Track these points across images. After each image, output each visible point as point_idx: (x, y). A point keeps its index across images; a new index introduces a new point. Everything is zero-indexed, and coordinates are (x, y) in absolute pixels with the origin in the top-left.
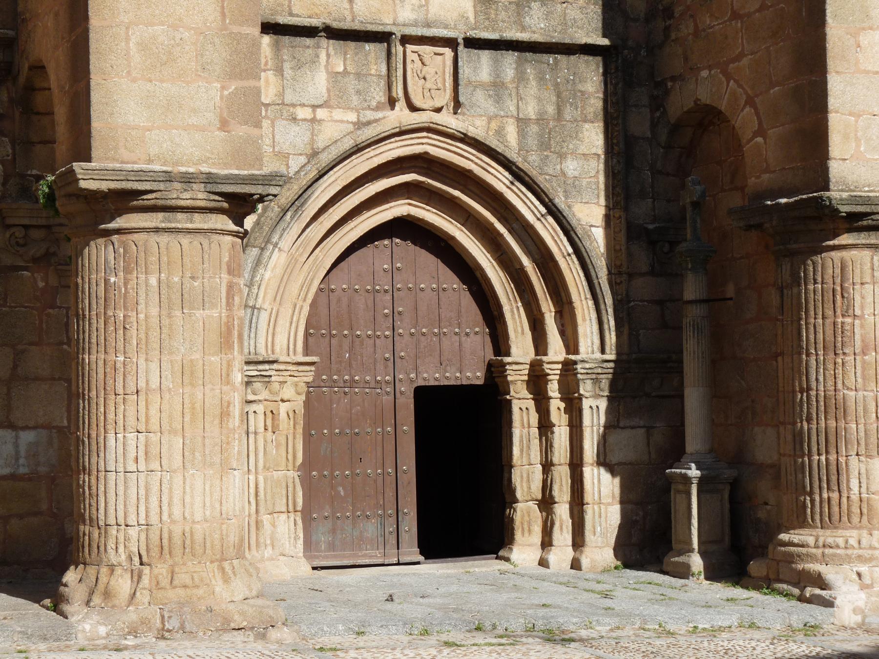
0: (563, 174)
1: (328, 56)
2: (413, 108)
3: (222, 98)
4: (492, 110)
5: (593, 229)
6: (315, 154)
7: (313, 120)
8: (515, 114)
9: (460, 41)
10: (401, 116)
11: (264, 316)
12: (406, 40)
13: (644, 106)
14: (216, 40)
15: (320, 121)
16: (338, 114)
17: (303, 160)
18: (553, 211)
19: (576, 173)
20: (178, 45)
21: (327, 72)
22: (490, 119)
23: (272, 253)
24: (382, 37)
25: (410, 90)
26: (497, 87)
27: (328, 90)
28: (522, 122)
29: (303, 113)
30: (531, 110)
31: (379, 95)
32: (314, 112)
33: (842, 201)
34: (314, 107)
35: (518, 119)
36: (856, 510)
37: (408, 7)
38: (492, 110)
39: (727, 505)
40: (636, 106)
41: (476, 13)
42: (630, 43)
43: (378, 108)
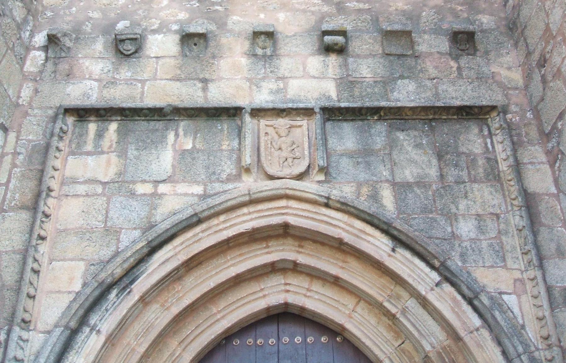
1: (177, 135)
4: (363, 176)
5: (505, 297)
7: (155, 195)
8: (390, 178)
9: (317, 110)
10: (252, 184)
12: (257, 112)
13: (542, 163)
15: (161, 196)
16: (182, 188)
18: (448, 277)
19: (473, 235)
21: (175, 150)
22: (360, 185)
23: (88, 337)
24: (232, 113)
25: (263, 159)
26: (364, 154)
27: (173, 166)
28: (401, 188)
29: (142, 189)
30: (408, 174)
31: (228, 168)
32: (156, 187)
34: (157, 183)
35: (394, 184)
38: (363, 176)
40: (531, 163)
41: (339, 92)
42: (513, 108)
43: (229, 179)
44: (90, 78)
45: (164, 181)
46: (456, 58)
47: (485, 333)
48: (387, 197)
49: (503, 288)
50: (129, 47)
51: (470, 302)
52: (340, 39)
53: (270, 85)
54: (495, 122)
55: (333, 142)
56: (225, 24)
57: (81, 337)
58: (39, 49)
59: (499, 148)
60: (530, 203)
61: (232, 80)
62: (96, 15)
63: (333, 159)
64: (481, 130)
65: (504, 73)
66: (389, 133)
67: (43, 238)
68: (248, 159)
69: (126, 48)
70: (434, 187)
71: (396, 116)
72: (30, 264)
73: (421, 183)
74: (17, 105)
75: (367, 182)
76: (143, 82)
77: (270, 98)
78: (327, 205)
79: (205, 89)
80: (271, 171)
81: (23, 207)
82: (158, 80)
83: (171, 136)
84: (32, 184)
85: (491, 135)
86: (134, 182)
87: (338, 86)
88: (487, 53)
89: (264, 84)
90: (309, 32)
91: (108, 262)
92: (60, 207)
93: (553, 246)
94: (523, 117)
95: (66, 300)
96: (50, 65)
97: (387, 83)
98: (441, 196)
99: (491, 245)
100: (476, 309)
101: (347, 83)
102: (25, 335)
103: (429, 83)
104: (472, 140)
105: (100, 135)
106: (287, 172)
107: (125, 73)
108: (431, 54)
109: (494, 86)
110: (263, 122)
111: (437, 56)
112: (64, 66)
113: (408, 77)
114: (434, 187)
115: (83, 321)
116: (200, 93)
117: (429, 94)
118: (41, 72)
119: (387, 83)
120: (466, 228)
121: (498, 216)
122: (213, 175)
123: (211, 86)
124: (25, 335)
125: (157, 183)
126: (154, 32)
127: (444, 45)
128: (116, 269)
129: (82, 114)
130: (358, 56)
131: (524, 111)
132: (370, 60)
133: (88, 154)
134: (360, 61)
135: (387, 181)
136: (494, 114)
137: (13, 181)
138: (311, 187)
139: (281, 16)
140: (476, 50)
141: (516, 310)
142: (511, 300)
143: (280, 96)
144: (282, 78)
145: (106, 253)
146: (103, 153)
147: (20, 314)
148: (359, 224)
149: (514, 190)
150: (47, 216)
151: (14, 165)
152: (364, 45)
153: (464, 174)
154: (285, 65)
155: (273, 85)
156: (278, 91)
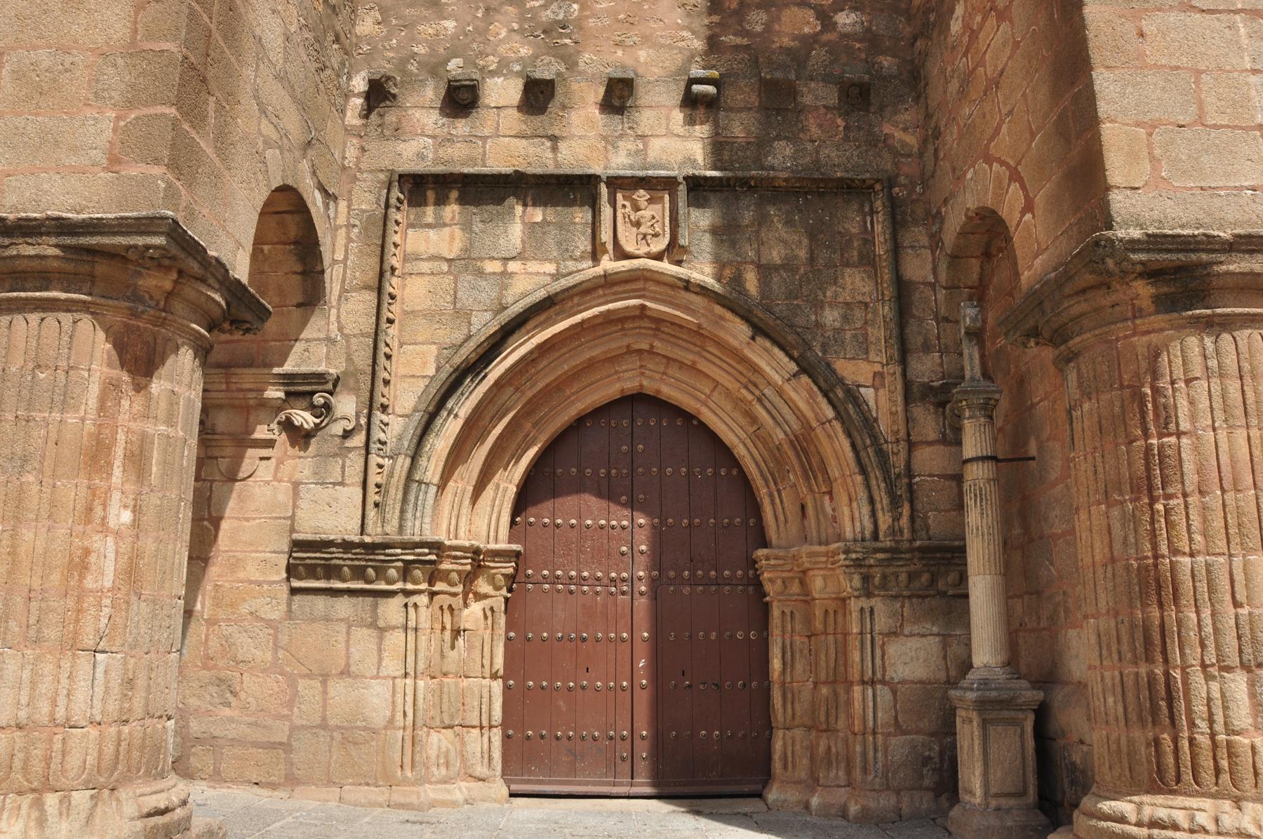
0: (818, 324)
2: (621, 254)
3: (115, 130)
5: (862, 390)
7: (504, 274)
8: (756, 259)
9: (680, 180)
13: (924, 247)
14: (120, 61)
15: (511, 275)
16: (533, 266)
18: (806, 368)
19: (837, 325)
20: (66, 71)
21: (524, 223)
23: (446, 420)
25: (620, 235)
27: (523, 242)
28: (765, 271)
30: (775, 255)
31: (584, 244)
32: (505, 265)
33: (1133, 245)
34: (506, 260)
36: (1207, 762)
37: (623, 153)
38: (726, 256)
39: (1030, 744)
40: (912, 247)
42: (902, 179)
46: (846, 115)
47: (837, 425)
48: (751, 282)
49: (862, 380)
50: (464, 96)
51: (826, 395)
53: (628, 145)
56: (576, 64)
57: (439, 421)
58: (358, 95)
59: (878, 228)
60: (903, 291)
61: (585, 141)
62: (421, 49)
64: (862, 206)
65: (898, 134)
67: (390, 321)
70: (802, 271)
73: (788, 266)
74: (344, 168)
75: (730, 263)
76: (484, 139)
78: (687, 289)
79: (555, 149)
81: (367, 287)
85: (872, 212)
86: (481, 259)
89: (621, 143)
92: (404, 286)
93: (920, 340)
95: (422, 384)
97: (762, 144)
99: (855, 336)
100: (830, 402)
102: (385, 418)
103: (809, 146)
107: (462, 127)
108: (817, 108)
109: (886, 154)
111: (822, 111)
112: (391, 118)
113: (786, 138)
114: (802, 271)
116: (551, 155)
117: (808, 159)
119: (762, 144)
120: (831, 317)
121: (866, 305)
123: (562, 145)
124: (385, 418)
125: (506, 260)
126: (493, 74)
127: (831, 96)
130: (731, 109)
131: (914, 184)
132: (743, 115)
133: (429, 226)
134: (732, 115)
135: (752, 262)
137: (351, 257)
140: (869, 104)
141: (872, 403)
142: (868, 393)
143: (639, 160)
144: (642, 137)
145: (458, 336)
146: (445, 225)
149: (887, 275)
150: (392, 297)
151: (349, 240)
153: (837, 256)
154: (646, 119)
156: (637, 152)
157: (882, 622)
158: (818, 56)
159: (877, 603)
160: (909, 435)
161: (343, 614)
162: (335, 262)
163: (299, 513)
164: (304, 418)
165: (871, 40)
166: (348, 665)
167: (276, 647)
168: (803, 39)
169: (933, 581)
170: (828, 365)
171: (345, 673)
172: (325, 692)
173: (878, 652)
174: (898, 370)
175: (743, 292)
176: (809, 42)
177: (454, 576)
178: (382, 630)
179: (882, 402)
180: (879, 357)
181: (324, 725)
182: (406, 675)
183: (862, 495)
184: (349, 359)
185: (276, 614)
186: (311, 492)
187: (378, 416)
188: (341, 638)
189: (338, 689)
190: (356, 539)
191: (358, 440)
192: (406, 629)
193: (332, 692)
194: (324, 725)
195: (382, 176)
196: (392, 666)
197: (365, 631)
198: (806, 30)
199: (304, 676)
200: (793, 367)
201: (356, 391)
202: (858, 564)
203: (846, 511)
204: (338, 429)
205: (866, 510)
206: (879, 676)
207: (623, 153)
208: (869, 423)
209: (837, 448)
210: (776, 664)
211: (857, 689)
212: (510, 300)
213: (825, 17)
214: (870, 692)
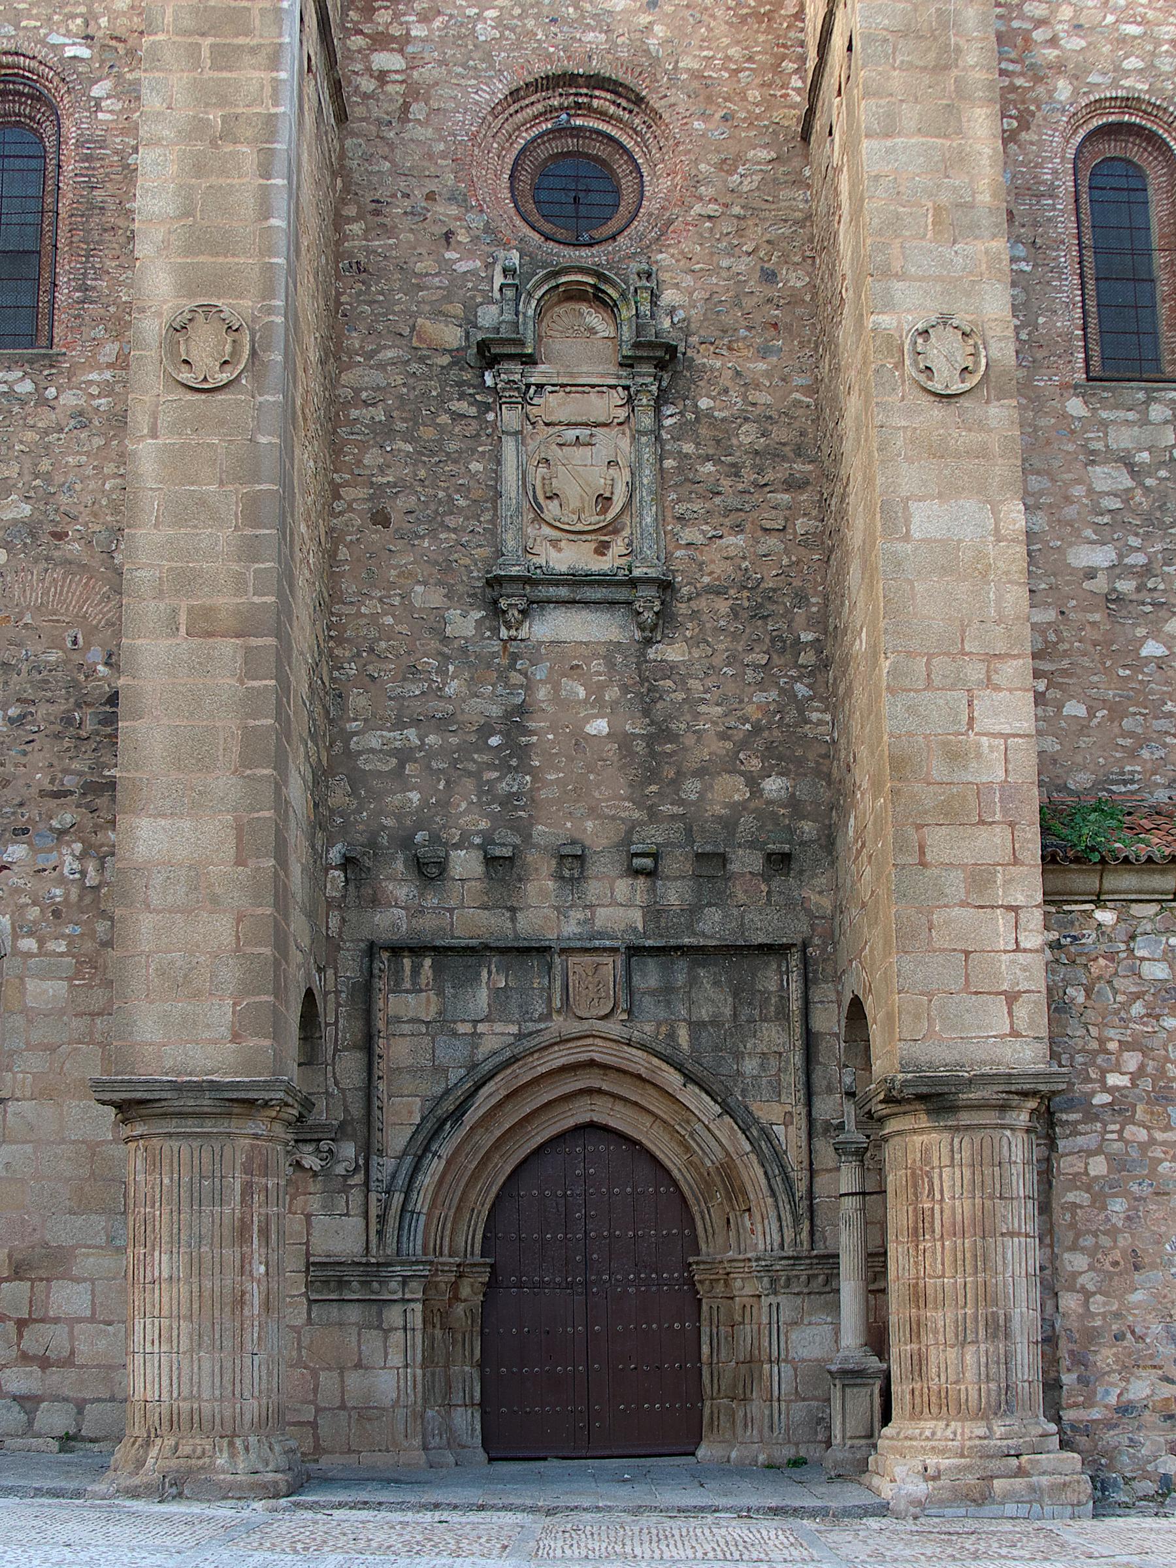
1: (490, 972)
4: (662, 1015)
6: (475, 1066)
11: (423, 1218)
16: (499, 1027)
17: (463, 1072)
18: (727, 1110)
19: (755, 1072)
22: (659, 1024)
26: (666, 992)
28: (696, 1027)
29: (462, 1028)
30: (704, 1014)
32: (475, 1027)
35: (690, 1023)
37: (573, 922)
40: (822, 1002)
41: (644, 922)
43: (542, 1018)
44: (397, 906)
45: (481, 1021)
46: (767, 879)
47: (753, 1157)
52: (648, 862)
53: (577, 915)
54: (795, 959)
55: (636, 979)
58: (335, 868)
59: (793, 986)
60: (810, 1041)
61: (541, 911)
62: (389, 822)
63: (637, 997)
64: (779, 966)
65: (814, 898)
66: (691, 969)
68: (557, 1003)
69: (429, 871)
71: (699, 954)
72: (377, 1103)
73: (715, 1022)
77: (578, 930)
79: (513, 920)
80: (579, 1014)
81: (355, 1047)
82: (466, 913)
83: (485, 974)
84: (359, 1025)
85: (787, 972)
86: (455, 1022)
87: (644, 916)
88: (801, 872)
90: (617, 845)
91: (441, 1097)
92: (389, 1046)
93: (825, 1083)
94: (824, 950)
96: (351, 888)
97: (694, 911)
98: (732, 1035)
99: (770, 1082)
101: (653, 912)
103: (735, 912)
104: (769, 979)
105: (416, 971)
106: (594, 1012)
107: (432, 901)
108: (743, 875)
109: (802, 915)
110: (572, 960)
111: (748, 877)
115: (427, 1149)
118: (344, 897)
119: (694, 911)
120: (750, 1066)
121: (780, 1054)
122: (525, 1015)
126: (457, 846)
128: (449, 1105)
129: (396, 951)
132: (679, 883)
133: (407, 991)
136: (794, 950)
137: (341, 1021)
138: (613, 1028)
139: (589, 825)
140: (790, 869)
141: (782, 1139)
142: (779, 1130)
143: (587, 927)
144: (590, 906)
145: (439, 1090)
146: (421, 991)
147: (376, 1146)
148: (656, 1061)
150: (380, 1057)
151: (338, 1005)
152: (676, 864)
153: (757, 1012)
154: (594, 889)
155: (580, 916)
157: (786, 1315)
158: (747, 822)
159: (780, 1299)
160: (811, 1164)
161: (353, 1319)
162: (327, 1025)
163: (312, 1239)
164: (311, 1161)
165: (793, 802)
166: (360, 1360)
167: (299, 1348)
168: (733, 806)
169: (827, 1282)
170: (746, 1108)
171: (359, 1366)
172: (343, 1381)
173: (782, 1338)
174: (804, 1112)
175: (677, 1047)
176: (738, 809)
177: (443, 1286)
178: (387, 1332)
179: (790, 1138)
180: (792, 1100)
181: (343, 1407)
182: (406, 1366)
183: (773, 1214)
184: (346, 1110)
185: (300, 1321)
186: (320, 1221)
187: (375, 1160)
188: (354, 1338)
189: (353, 1379)
190: (364, 1260)
191: (358, 1179)
192: (405, 1329)
193: (348, 1381)
194: (343, 1407)
195: (362, 945)
196: (396, 1359)
197: (374, 1332)
198: (736, 797)
199: (323, 1369)
200: (718, 1109)
201: (353, 1137)
202: (767, 1269)
203: (760, 1228)
204: (340, 1169)
205: (775, 1226)
206: (783, 1356)
207: (573, 922)
208: (778, 1155)
209: (753, 1174)
210: (705, 1349)
211: (766, 1366)
212: (480, 1057)
213: (753, 782)
214: (776, 1369)
